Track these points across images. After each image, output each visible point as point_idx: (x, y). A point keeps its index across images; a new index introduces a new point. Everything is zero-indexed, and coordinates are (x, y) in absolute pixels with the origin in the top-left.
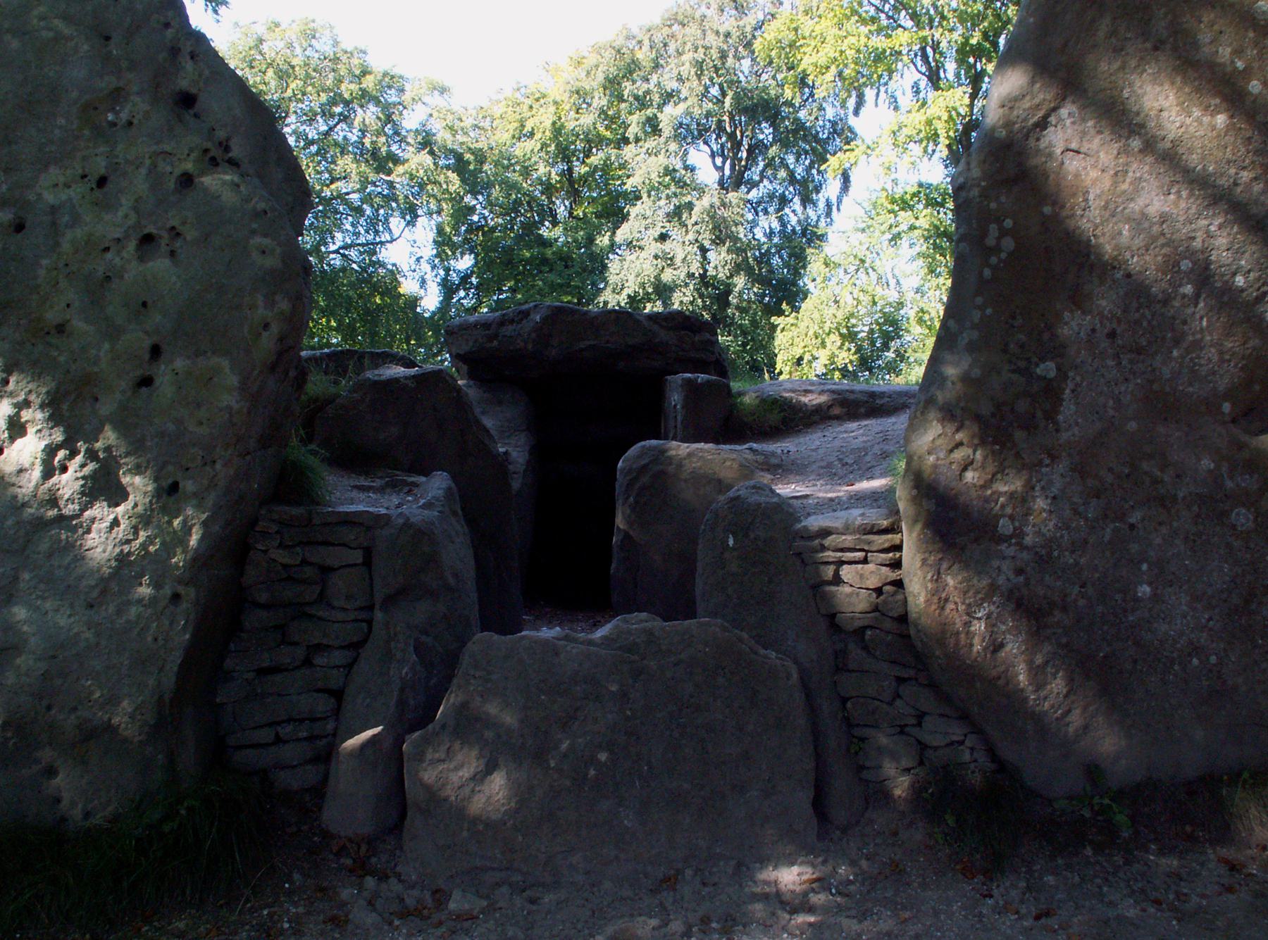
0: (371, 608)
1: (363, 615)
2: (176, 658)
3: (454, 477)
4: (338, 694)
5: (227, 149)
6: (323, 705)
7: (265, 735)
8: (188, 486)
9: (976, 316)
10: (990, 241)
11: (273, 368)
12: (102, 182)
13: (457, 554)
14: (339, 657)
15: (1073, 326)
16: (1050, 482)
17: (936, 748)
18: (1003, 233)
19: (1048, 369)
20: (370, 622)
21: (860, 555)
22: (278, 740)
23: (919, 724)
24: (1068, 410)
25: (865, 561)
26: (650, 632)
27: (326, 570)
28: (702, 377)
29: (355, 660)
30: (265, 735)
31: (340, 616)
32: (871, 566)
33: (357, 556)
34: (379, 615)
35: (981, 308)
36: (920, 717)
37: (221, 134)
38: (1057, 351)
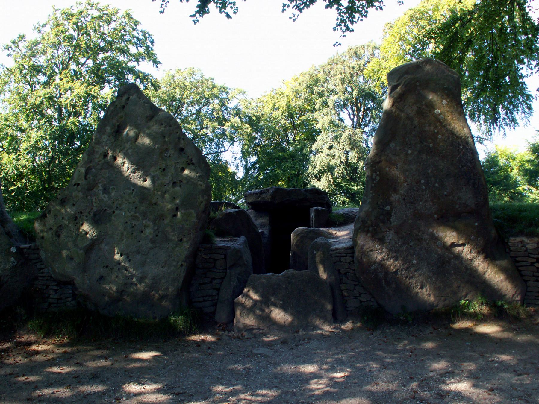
0: (226, 269)
1: (224, 271)
2: (182, 279)
3: (246, 238)
4: (218, 290)
5: (192, 161)
6: (215, 292)
7: (201, 299)
8: (185, 239)
9: (371, 195)
10: (374, 177)
11: (203, 212)
12: (164, 170)
13: (247, 256)
14: (218, 281)
15: (394, 197)
16: (389, 236)
17: (364, 302)
18: (377, 175)
19: (388, 208)
20: (226, 273)
21: (345, 255)
22: (204, 301)
23: (360, 296)
24: (393, 218)
25: (346, 256)
26: (293, 273)
27: (215, 260)
28: (320, 208)
29: (223, 281)
30: (201, 299)
31: (219, 271)
32: (348, 257)
33: (223, 257)
34: (228, 271)
35: (372, 194)
36: (360, 294)
37: (190, 157)
38: (390, 204)
